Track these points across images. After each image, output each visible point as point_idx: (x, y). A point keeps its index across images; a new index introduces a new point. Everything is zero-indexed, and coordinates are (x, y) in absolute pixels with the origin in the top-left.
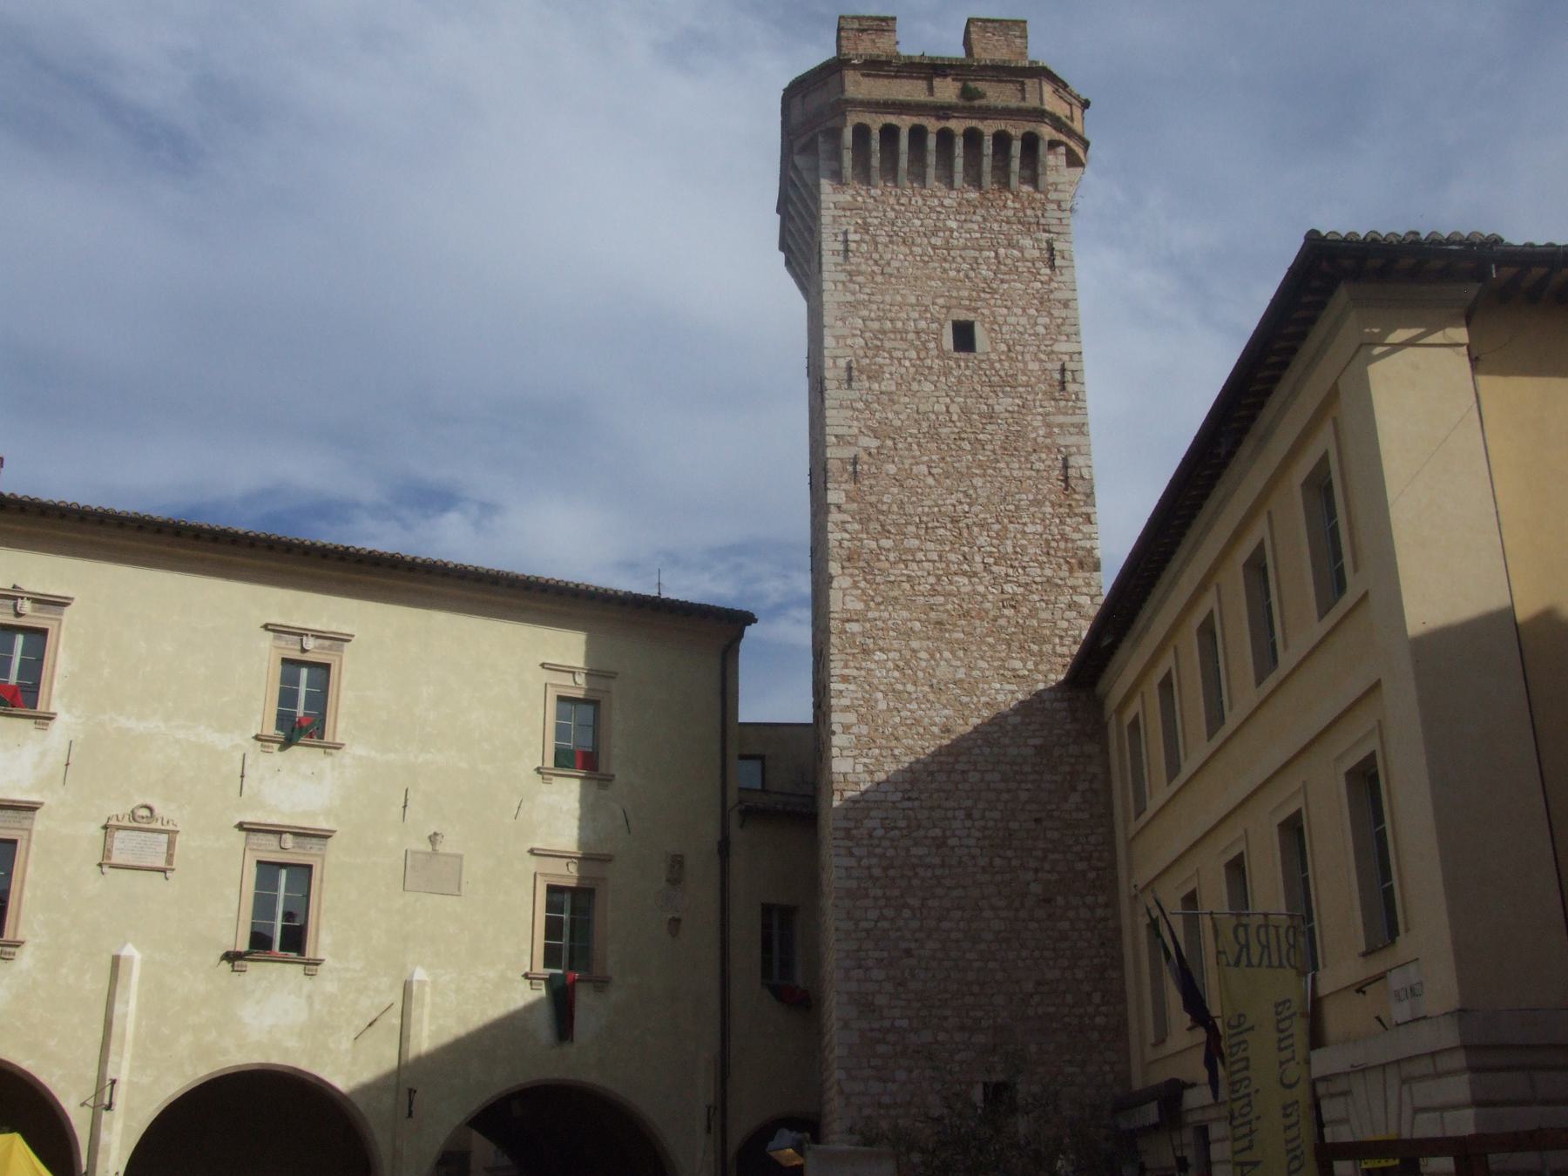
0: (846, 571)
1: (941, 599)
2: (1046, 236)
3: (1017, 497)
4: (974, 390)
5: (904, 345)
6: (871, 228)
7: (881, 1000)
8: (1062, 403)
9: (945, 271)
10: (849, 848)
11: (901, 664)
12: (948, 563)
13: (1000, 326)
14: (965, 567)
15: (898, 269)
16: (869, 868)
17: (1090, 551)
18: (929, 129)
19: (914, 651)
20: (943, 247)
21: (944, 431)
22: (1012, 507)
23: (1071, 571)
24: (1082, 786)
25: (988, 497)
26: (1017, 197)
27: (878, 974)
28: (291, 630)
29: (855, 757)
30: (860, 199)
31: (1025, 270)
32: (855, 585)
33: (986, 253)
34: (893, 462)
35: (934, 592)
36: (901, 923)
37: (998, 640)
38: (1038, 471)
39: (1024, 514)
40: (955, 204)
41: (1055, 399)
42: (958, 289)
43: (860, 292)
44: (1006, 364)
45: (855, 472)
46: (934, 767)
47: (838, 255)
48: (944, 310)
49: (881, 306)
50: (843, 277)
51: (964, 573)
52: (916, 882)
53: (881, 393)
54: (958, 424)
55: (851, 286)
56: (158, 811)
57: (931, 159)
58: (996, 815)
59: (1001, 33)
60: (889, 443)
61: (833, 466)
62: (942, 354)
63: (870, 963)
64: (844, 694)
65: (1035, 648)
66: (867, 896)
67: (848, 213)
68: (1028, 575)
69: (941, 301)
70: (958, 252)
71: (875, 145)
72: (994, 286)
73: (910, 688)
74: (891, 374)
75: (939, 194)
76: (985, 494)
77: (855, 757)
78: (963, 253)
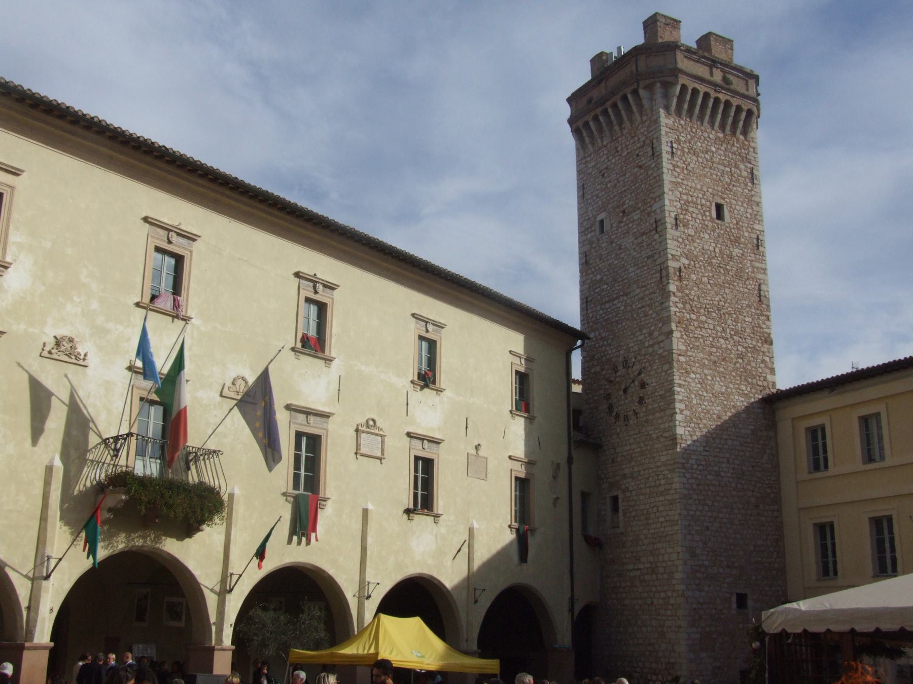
0: (679, 329)
1: (714, 350)
2: (749, 165)
3: (742, 302)
4: (724, 242)
5: (697, 211)
7: (698, 551)
8: (758, 256)
10: (684, 473)
11: (701, 381)
12: (717, 331)
13: (734, 210)
14: (724, 335)
16: (692, 484)
17: (769, 334)
18: (712, 96)
19: (705, 375)
21: (714, 261)
22: (739, 307)
23: (762, 343)
24: (768, 451)
25: (731, 300)
26: (738, 140)
27: (697, 538)
28: (422, 318)
29: (684, 427)
32: (682, 337)
34: (694, 274)
35: (712, 346)
36: (704, 513)
37: (736, 374)
38: (749, 290)
39: (744, 311)
41: (755, 254)
42: (717, 186)
44: (736, 231)
45: (680, 276)
46: (714, 436)
48: (712, 196)
50: (671, 167)
51: (723, 338)
52: (709, 493)
53: (689, 235)
54: (719, 259)
56: (378, 424)
58: (738, 462)
60: (692, 263)
61: (671, 271)
62: (711, 220)
64: (680, 393)
65: (750, 380)
66: (691, 498)
67: (672, 131)
68: (747, 343)
69: (710, 190)
70: (716, 165)
73: (705, 394)
74: (692, 226)
76: (730, 298)
77: (684, 427)
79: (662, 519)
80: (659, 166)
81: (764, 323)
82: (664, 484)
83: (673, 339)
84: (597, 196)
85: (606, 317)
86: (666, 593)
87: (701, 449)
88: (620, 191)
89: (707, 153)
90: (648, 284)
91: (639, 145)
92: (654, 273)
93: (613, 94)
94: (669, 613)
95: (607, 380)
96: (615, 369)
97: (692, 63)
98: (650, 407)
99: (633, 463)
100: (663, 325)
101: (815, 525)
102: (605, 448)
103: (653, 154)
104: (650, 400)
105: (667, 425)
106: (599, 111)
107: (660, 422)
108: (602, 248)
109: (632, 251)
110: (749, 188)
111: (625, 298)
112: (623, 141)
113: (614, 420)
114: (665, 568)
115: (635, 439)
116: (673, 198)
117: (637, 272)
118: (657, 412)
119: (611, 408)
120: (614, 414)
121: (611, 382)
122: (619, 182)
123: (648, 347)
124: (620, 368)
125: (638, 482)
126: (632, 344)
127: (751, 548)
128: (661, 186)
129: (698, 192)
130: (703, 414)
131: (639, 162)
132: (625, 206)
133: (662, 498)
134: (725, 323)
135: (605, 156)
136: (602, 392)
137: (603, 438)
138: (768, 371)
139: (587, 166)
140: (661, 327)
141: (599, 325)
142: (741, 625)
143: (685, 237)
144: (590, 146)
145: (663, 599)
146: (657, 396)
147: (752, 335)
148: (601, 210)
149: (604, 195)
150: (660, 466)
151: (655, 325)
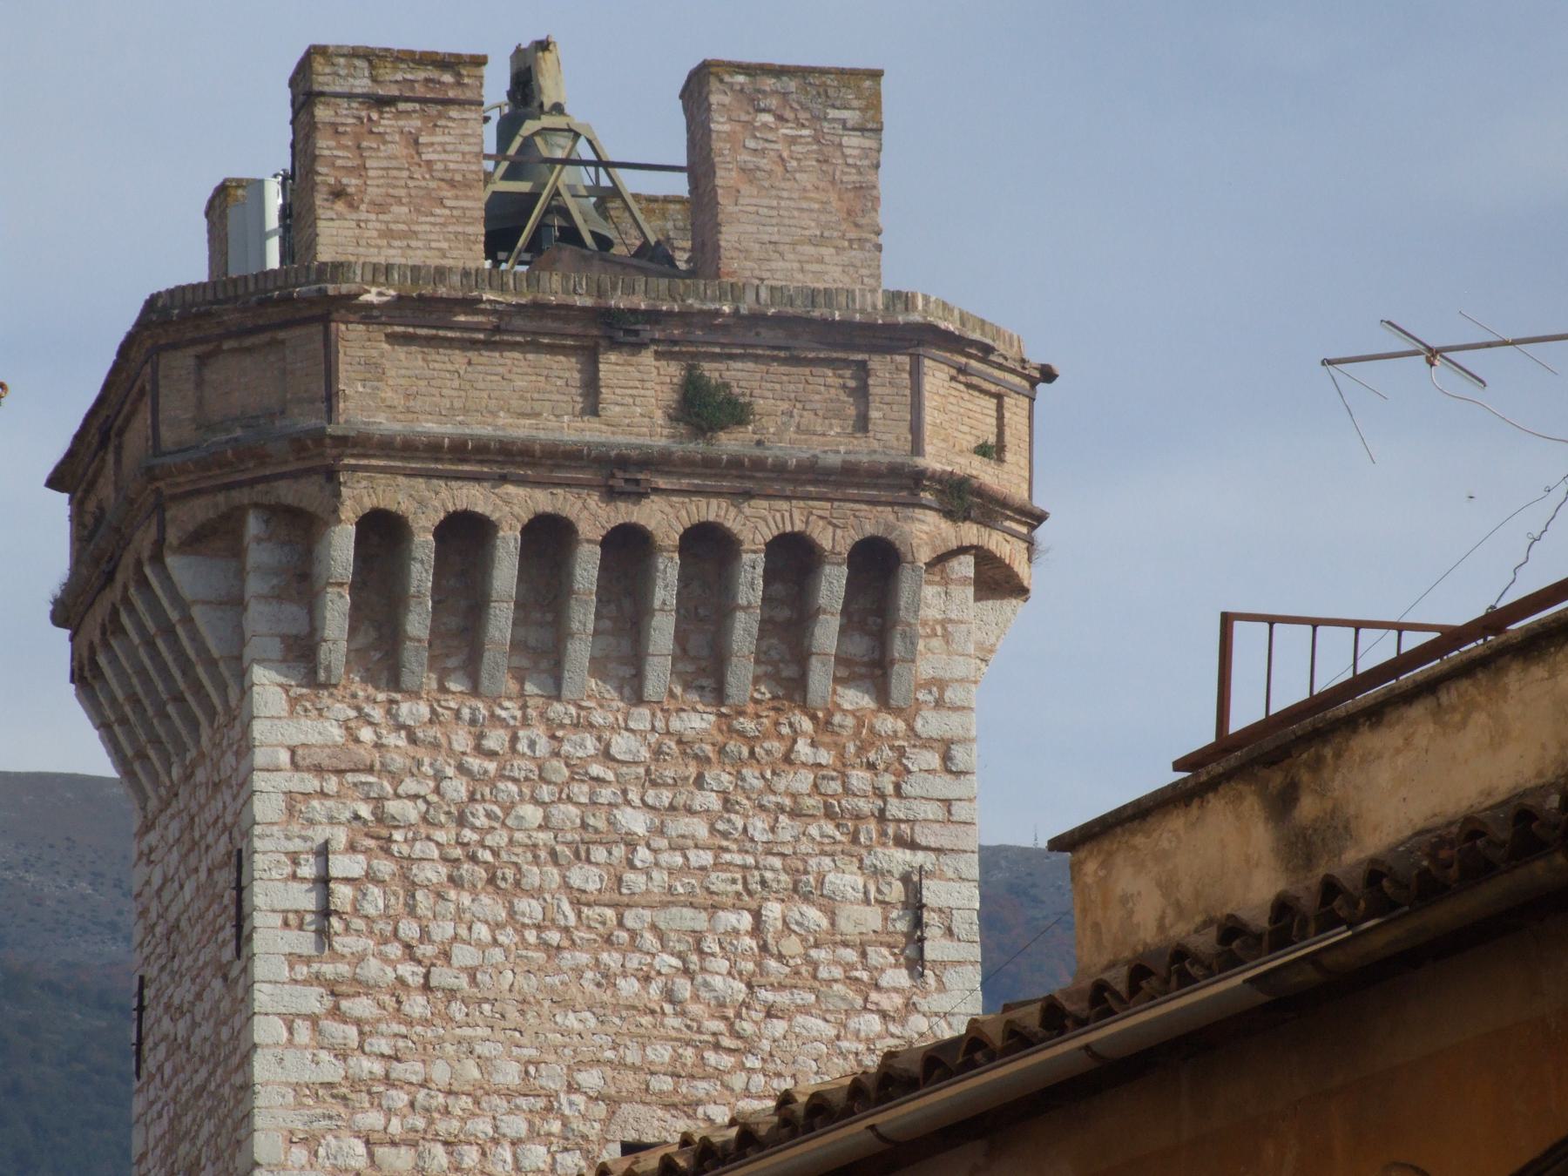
2: (901, 858)
6: (398, 836)
20: (606, 897)
26: (824, 725)
30: (366, 734)
31: (838, 973)
33: (728, 919)
40: (645, 754)
43: (361, 1047)
47: (301, 927)
48: (601, 1110)
49: (423, 1092)
50: (313, 1000)
55: (331, 1027)
57: (583, 616)
59: (803, 115)
67: (332, 784)
69: (590, 1079)
70: (647, 913)
71: (421, 574)
72: (747, 1027)
75: (598, 718)
78: (662, 919)
89: (581, 855)
110: (891, 1002)
129: (502, 1104)
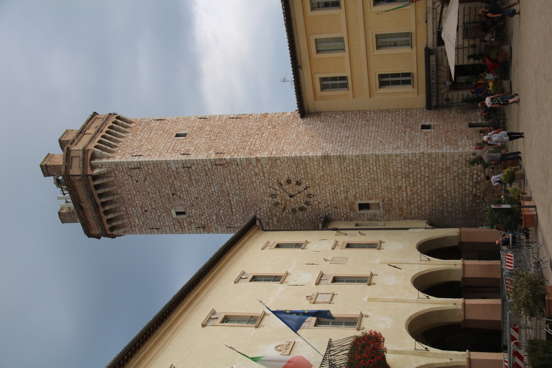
3: (240, 126)
5: (180, 146)
7: (395, 146)
9: (156, 138)
14: (260, 134)
15: (151, 147)
21: (213, 138)
22: (243, 127)
27: (387, 147)
46: (323, 139)
56: (310, 295)
60: (213, 148)
61: (217, 157)
63: (383, 148)
66: (362, 149)
69: (166, 139)
73: (297, 143)
74: (189, 148)
79: (375, 168)
80: (147, 164)
81: (254, 117)
82: (353, 166)
83: (261, 156)
84: (159, 217)
85: (242, 211)
86: (422, 166)
87: (331, 145)
88: (159, 197)
90: (224, 175)
91: (130, 180)
92: (217, 171)
93: (92, 196)
94: (434, 164)
95: (283, 212)
96: (277, 204)
97: (80, 143)
98: (303, 176)
99: (338, 191)
100: (252, 165)
101: (380, 87)
102: (327, 214)
103: (139, 168)
104: (299, 176)
105: (315, 163)
106: (102, 210)
107: (312, 168)
108: (195, 214)
109: (200, 188)
111: (231, 195)
112: (126, 193)
113: (310, 206)
114: (406, 166)
115: (323, 189)
116: (169, 156)
117: (214, 184)
118: (306, 171)
119: (301, 209)
120: (305, 206)
121: (285, 208)
122: (153, 198)
123: (265, 177)
124: (276, 200)
125: (351, 186)
126: (262, 189)
127: (393, 123)
128: (161, 163)
130: (310, 144)
131: (142, 180)
132: (170, 194)
133: (361, 168)
134: (253, 133)
135: (133, 209)
136: (290, 216)
137: (321, 216)
138: (284, 116)
139: (138, 225)
140: (253, 166)
141: (246, 217)
142: (441, 127)
143: (196, 151)
144: (124, 221)
145: (425, 168)
146: (297, 170)
147: (261, 122)
148: (170, 213)
149: (160, 211)
150: (341, 169)
151: (251, 171)
